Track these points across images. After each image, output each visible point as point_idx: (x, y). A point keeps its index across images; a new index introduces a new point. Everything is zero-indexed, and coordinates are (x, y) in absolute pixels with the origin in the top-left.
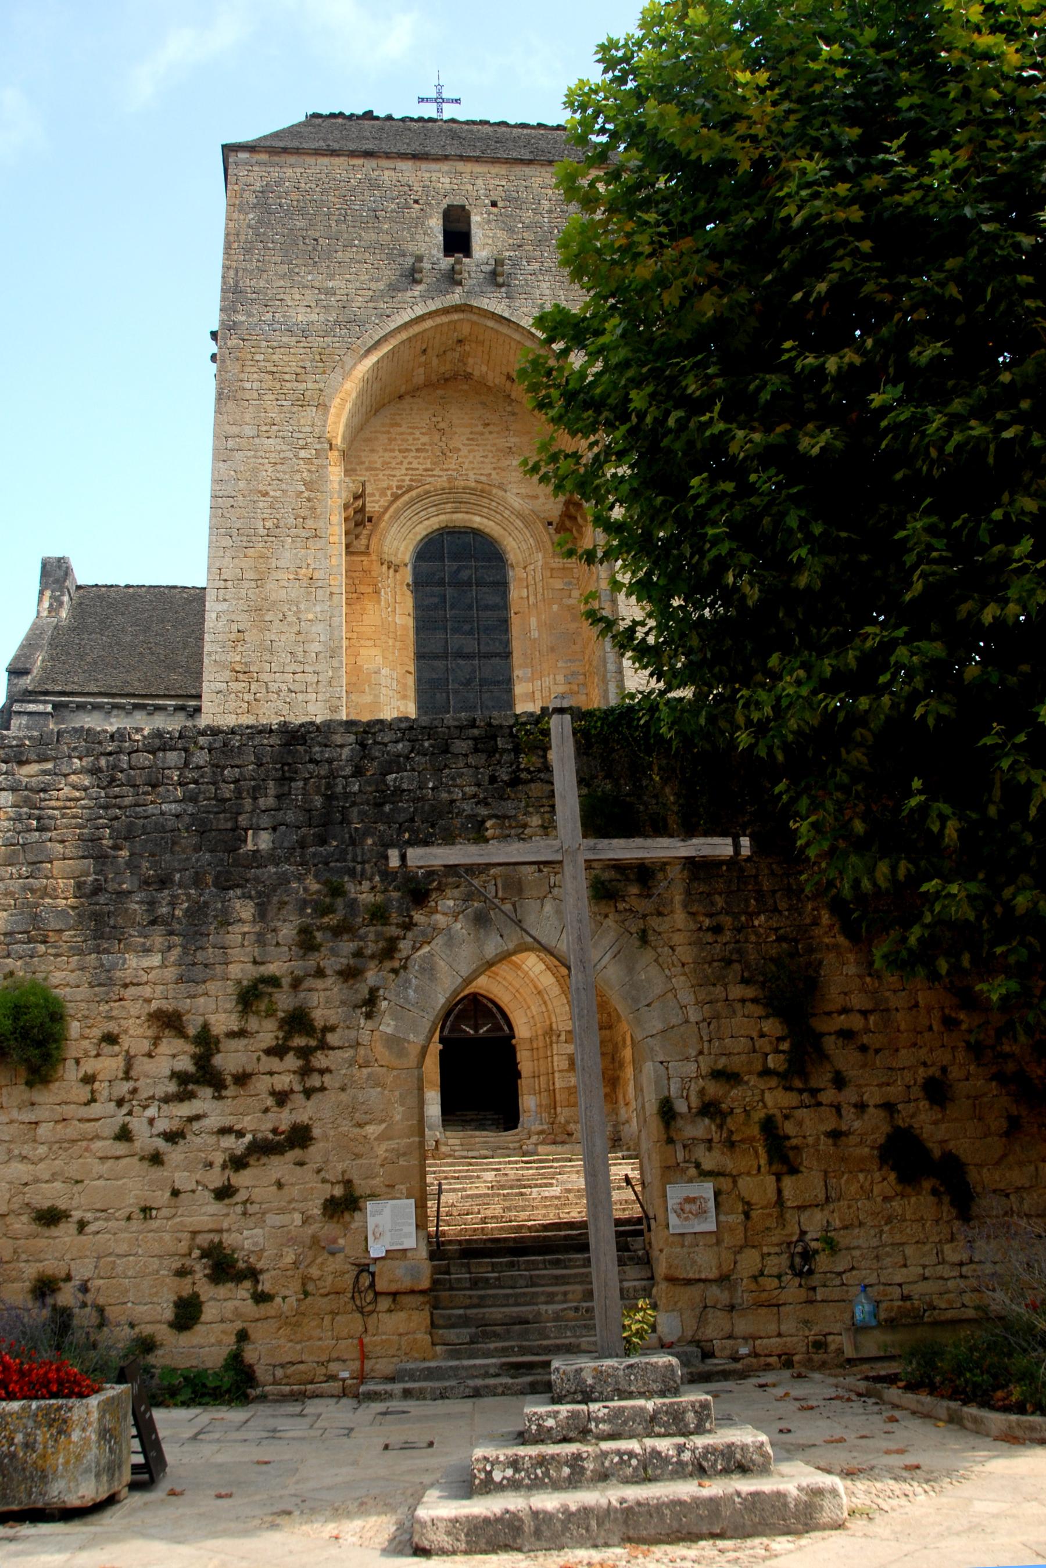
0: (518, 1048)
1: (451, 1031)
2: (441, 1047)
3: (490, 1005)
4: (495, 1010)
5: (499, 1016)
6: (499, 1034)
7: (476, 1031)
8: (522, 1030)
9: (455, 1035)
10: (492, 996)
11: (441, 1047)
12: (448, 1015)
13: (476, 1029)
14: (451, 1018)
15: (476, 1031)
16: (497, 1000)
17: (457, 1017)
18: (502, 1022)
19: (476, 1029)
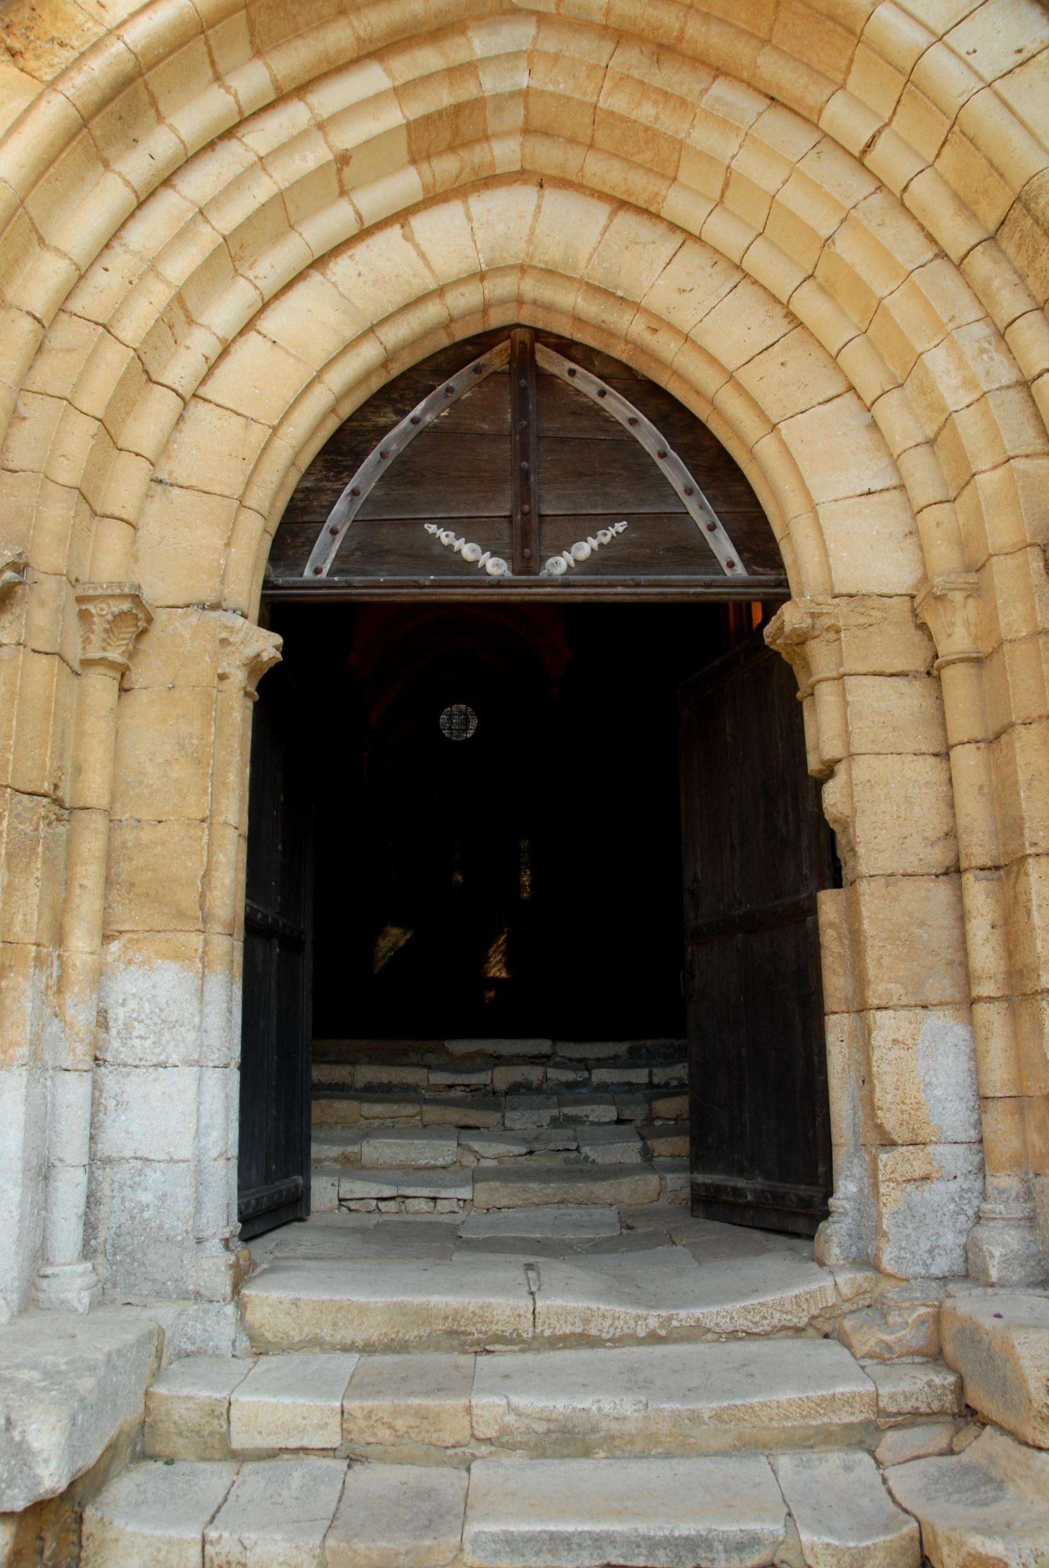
0: (821, 658)
1: (361, 551)
2: (268, 645)
3: (618, 407)
4: (649, 437)
5: (676, 473)
6: (675, 584)
7: (526, 563)
8: (846, 534)
9: (384, 583)
10: (635, 326)
11: (268, 645)
12: (341, 449)
13: (526, 545)
14: (366, 475)
15: (526, 563)
16: (667, 347)
17: (402, 473)
18: (699, 511)
19: (526, 545)
